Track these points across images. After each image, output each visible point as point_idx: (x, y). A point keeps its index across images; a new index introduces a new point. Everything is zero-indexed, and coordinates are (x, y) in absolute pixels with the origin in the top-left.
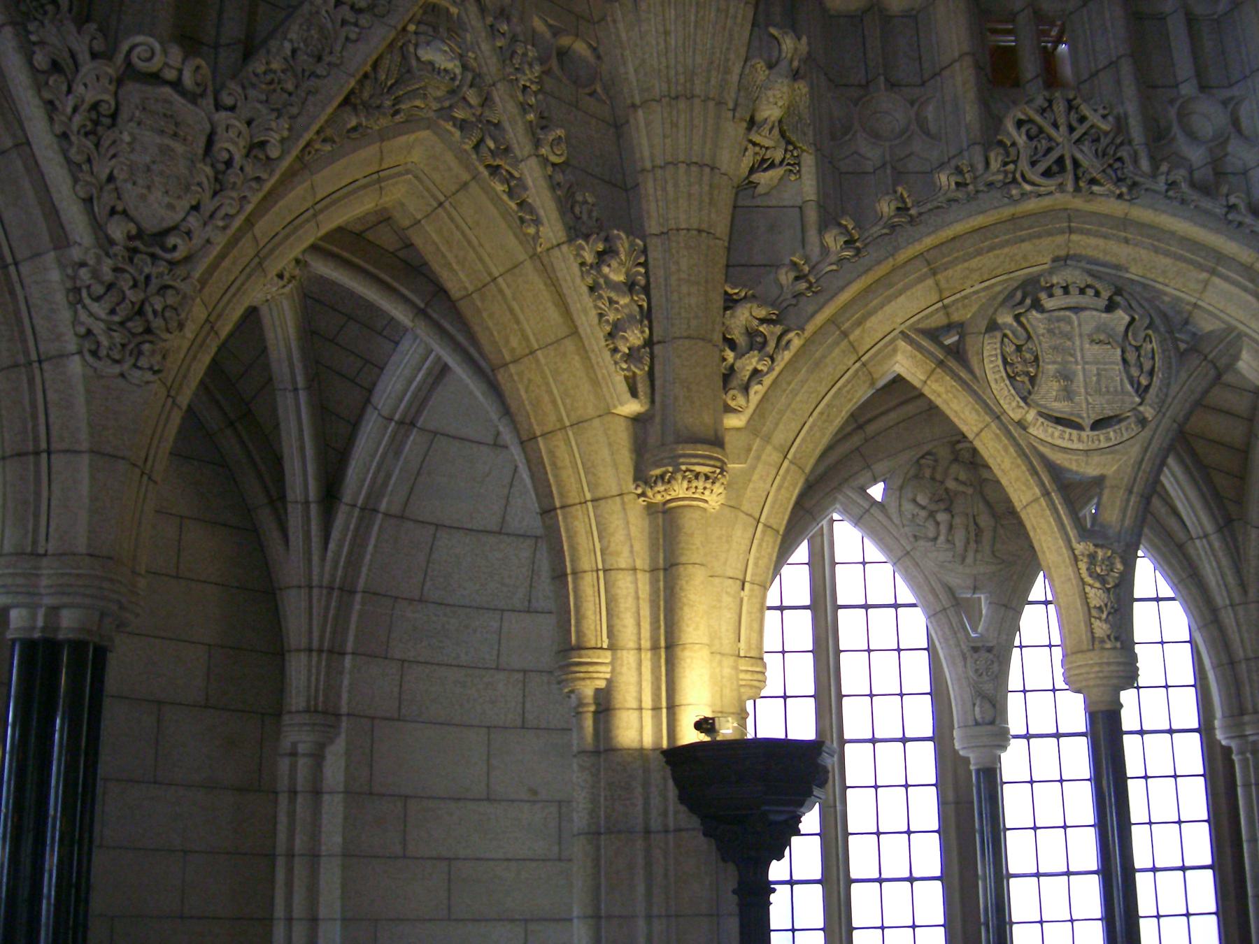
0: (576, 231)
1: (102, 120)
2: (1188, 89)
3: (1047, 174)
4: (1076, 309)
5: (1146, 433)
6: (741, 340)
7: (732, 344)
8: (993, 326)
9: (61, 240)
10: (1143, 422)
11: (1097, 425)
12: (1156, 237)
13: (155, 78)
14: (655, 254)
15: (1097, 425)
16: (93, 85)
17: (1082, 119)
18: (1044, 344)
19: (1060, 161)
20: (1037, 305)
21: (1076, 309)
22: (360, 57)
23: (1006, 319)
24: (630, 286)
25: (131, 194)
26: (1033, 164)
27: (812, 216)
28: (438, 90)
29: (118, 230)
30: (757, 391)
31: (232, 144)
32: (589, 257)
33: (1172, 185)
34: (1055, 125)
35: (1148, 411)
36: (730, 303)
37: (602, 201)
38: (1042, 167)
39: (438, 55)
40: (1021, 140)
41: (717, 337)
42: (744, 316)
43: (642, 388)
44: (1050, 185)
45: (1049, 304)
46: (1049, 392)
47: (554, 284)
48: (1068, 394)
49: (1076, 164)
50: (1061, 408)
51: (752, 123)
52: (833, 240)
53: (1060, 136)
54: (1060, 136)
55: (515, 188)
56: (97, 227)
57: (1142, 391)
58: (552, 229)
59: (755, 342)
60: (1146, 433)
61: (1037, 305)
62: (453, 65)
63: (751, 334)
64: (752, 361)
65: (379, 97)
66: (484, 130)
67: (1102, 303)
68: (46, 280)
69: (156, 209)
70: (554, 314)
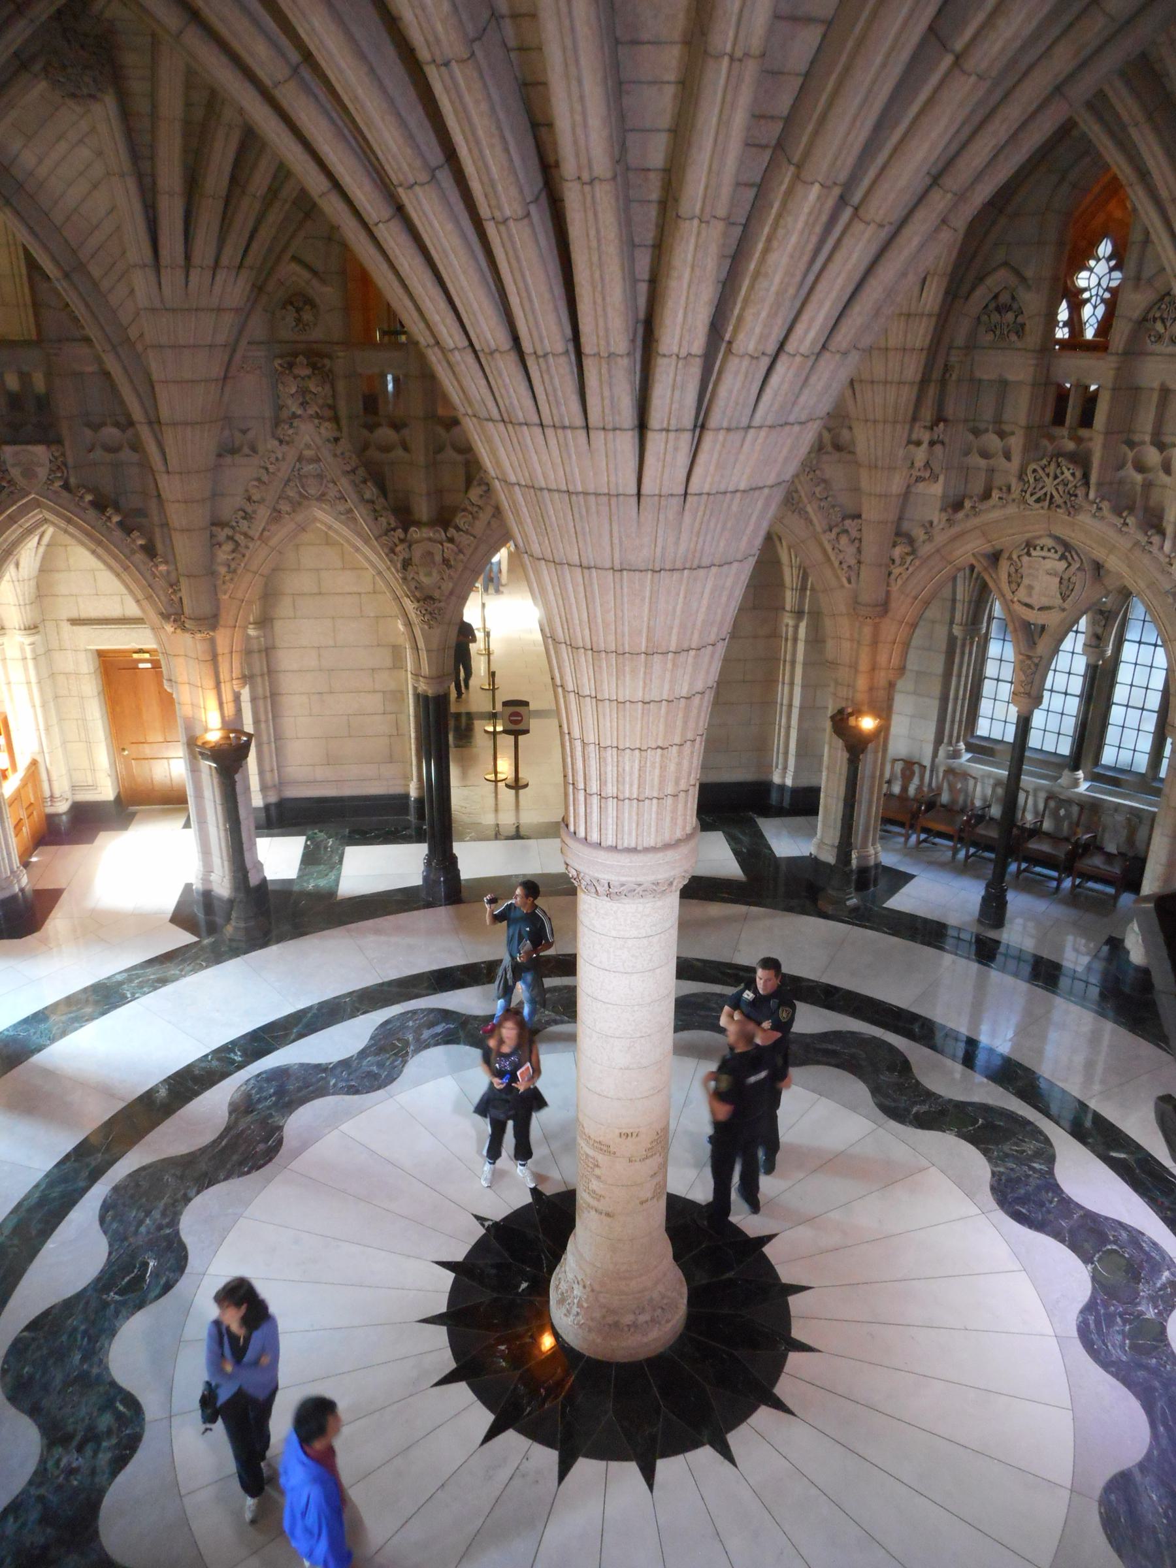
2: (1147, 438)
3: (1038, 501)
4: (1044, 558)
6: (898, 561)
7: (893, 561)
8: (1010, 558)
10: (1064, 610)
11: (1040, 609)
15: (1039, 609)
17: (1062, 473)
18: (1024, 571)
19: (1045, 494)
20: (1028, 554)
21: (1044, 558)
23: (1015, 557)
26: (1032, 495)
27: (938, 505)
32: (833, 535)
34: (1048, 475)
35: (1066, 605)
38: (1035, 497)
40: (1032, 480)
44: (1038, 506)
45: (1034, 553)
46: (1022, 594)
48: (1030, 595)
49: (1052, 497)
50: (1028, 600)
52: (944, 516)
53: (1048, 481)
54: (1048, 481)
61: (1028, 554)
67: (1057, 556)
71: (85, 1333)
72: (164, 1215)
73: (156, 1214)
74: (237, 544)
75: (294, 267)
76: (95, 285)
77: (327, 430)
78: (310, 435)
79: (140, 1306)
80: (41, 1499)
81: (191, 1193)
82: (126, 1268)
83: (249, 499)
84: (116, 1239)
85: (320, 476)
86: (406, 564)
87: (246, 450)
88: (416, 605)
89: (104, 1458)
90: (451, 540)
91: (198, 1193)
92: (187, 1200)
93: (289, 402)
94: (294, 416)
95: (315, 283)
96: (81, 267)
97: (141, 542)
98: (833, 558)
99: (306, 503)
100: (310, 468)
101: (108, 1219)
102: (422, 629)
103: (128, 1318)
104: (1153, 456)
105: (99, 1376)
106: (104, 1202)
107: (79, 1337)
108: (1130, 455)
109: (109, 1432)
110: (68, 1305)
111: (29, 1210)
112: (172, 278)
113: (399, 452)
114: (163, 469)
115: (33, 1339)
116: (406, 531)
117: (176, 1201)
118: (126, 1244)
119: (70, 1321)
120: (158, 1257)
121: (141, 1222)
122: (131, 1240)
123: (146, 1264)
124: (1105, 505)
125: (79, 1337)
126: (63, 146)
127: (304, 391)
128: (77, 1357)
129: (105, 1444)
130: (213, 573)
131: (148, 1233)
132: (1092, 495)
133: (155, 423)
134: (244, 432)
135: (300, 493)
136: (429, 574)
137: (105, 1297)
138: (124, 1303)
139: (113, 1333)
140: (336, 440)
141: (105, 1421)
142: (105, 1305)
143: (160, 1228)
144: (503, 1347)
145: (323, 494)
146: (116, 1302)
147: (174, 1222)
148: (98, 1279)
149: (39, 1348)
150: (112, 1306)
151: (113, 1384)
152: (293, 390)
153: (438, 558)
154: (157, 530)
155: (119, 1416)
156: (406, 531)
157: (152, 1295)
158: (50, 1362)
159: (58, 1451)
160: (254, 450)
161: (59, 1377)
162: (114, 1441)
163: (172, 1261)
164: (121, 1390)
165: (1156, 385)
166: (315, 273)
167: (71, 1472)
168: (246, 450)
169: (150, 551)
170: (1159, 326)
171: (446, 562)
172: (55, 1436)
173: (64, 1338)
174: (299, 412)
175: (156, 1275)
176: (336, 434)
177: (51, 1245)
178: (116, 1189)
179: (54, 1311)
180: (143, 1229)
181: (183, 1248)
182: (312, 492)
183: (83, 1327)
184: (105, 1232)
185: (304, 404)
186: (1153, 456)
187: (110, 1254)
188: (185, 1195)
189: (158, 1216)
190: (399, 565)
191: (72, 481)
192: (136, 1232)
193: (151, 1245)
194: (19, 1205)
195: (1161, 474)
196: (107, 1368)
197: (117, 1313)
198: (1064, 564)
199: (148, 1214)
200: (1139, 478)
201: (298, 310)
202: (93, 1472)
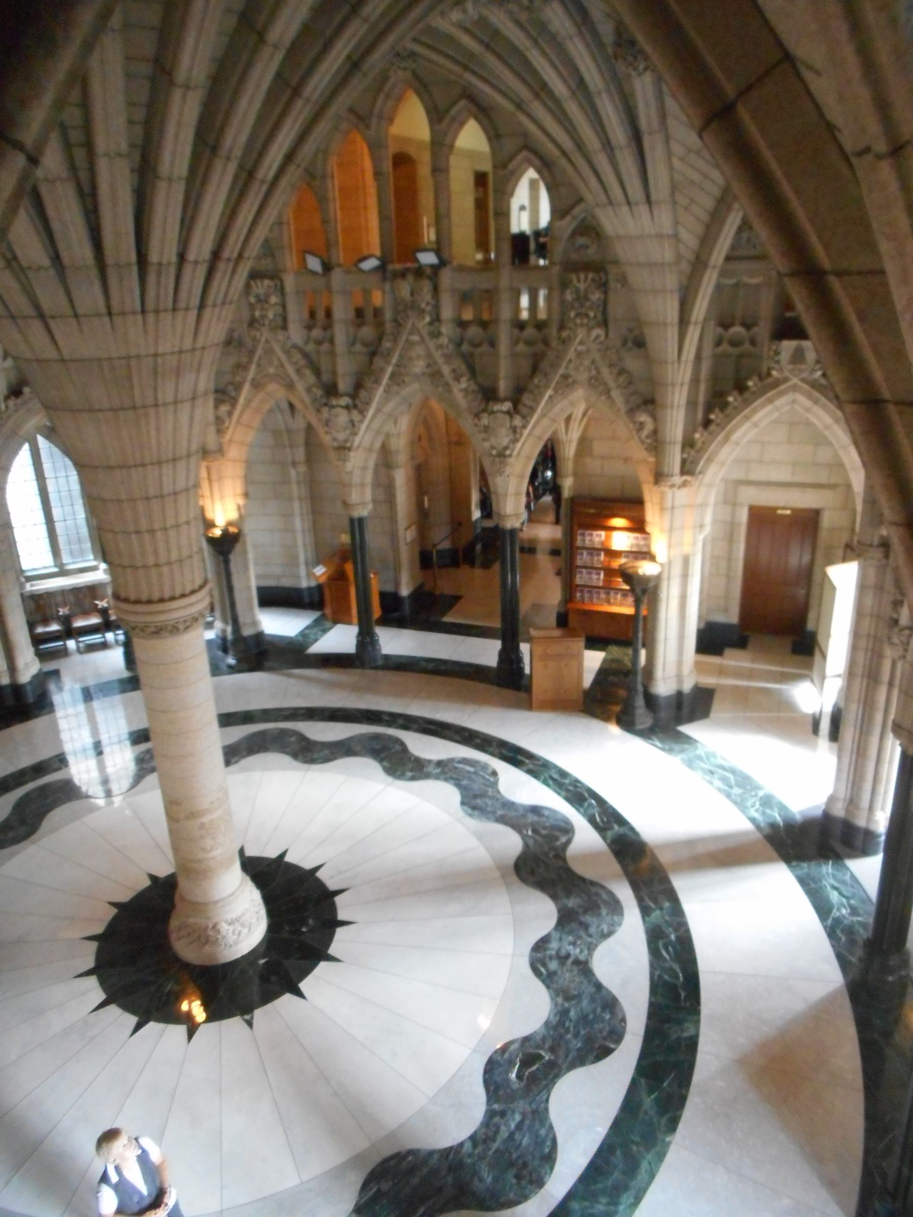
71: (567, 1031)
72: (497, 1132)
73: (504, 1133)
79: (526, 1039)
80: (590, 936)
81: (468, 1146)
82: (534, 1080)
84: (540, 1115)
89: (554, 945)
91: (461, 1144)
92: (473, 1138)
101: (549, 1143)
103: (535, 1032)
105: (557, 995)
106: (552, 1169)
107: (572, 1029)
109: (551, 958)
110: (581, 1060)
111: (626, 1188)
115: (605, 1039)
117: (485, 1141)
118: (534, 1106)
119: (579, 1045)
120: (507, 1081)
121: (519, 1126)
122: (529, 1110)
123: (519, 1077)
125: (572, 1029)
128: (572, 1014)
129: (553, 953)
131: (513, 1112)
137: (552, 1058)
138: (538, 1047)
139: (547, 1024)
141: (553, 965)
142: (552, 1050)
143: (503, 1114)
144: (304, 930)
146: (543, 1049)
147: (490, 1114)
148: (557, 1076)
149: (601, 1031)
150: (547, 1046)
151: (548, 987)
155: (544, 965)
157: (515, 1046)
158: (591, 1017)
159: (582, 957)
161: (585, 1003)
162: (548, 953)
163: (497, 1072)
164: (543, 981)
167: (574, 944)
172: (584, 968)
173: (583, 1032)
175: (511, 1063)
177: (601, 1130)
178: (540, 1183)
179: (591, 1058)
180: (518, 1117)
181: (487, 1083)
183: (569, 1036)
184: (551, 1127)
187: (547, 1100)
188: (475, 1146)
189: (503, 1128)
192: (524, 1115)
193: (511, 1097)
194: (638, 1199)
196: (552, 999)
197: (544, 1039)
199: (511, 1136)
202: (561, 939)
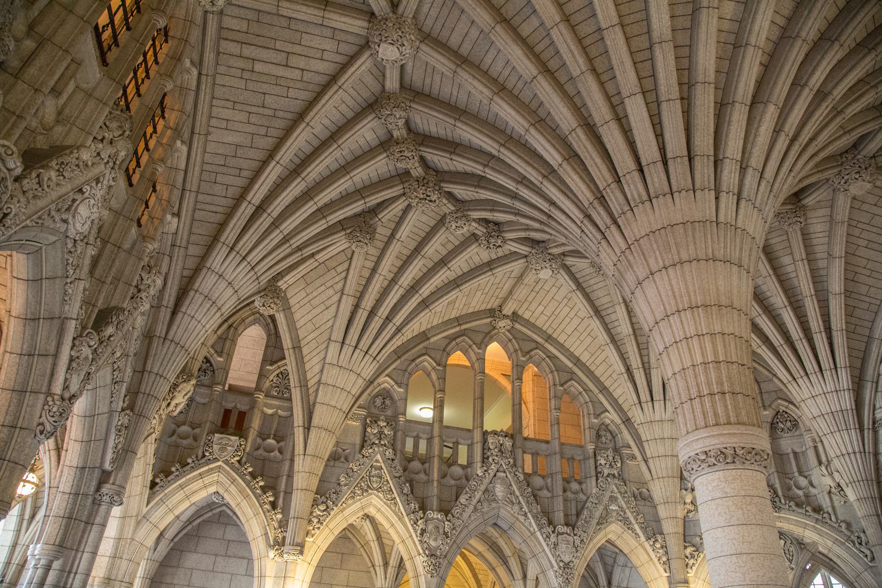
0: (648, 539)
1: (556, 545)
2: (796, 474)
5: (794, 572)
9: (552, 567)
10: (792, 569)
12: (788, 520)
13: (563, 533)
14: (667, 539)
16: (553, 538)
22: (597, 514)
24: (662, 547)
25: (562, 557)
28: (614, 514)
29: (561, 564)
30: (694, 568)
31: (578, 542)
32: (652, 543)
33: (790, 506)
36: (685, 547)
37: (653, 530)
39: (613, 507)
41: (683, 557)
42: (689, 550)
43: (668, 570)
47: (645, 550)
51: (685, 503)
55: (633, 530)
56: (558, 564)
57: (791, 561)
58: (643, 539)
59: (692, 556)
60: (794, 572)
62: (617, 508)
63: (691, 554)
64: (691, 562)
65: (603, 521)
66: (626, 521)
68: (551, 574)
69: (567, 559)
70: (646, 556)
74: (328, 507)
75: (387, 378)
76: (303, 358)
77: (389, 453)
78: (378, 457)
83: (339, 484)
85: (381, 477)
86: (423, 531)
87: (342, 459)
88: (426, 559)
90: (449, 521)
93: (372, 437)
94: (373, 444)
95: (396, 387)
96: (300, 348)
97: (272, 499)
98: (653, 557)
99: (370, 491)
100: (374, 472)
102: (426, 578)
104: (803, 482)
108: (792, 482)
112: (347, 350)
113: (422, 476)
114: (302, 452)
116: (424, 513)
124: (792, 503)
126: (323, 288)
127: (381, 433)
130: (310, 521)
132: (783, 501)
133: (307, 428)
134: (344, 451)
135: (368, 486)
136: (435, 540)
140: (393, 460)
145: (380, 488)
152: (375, 431)
153: (441, 531)
154: (282, 494)
156: (424, 513)
160: (347, 459)
165: (789, 451)
166: (396, 383)
168: (342, 459)
169: (274, 505)
170: (780, 425)
171: (445, 534)
174: (377, 442)
176: (393, 457)
182: (375, 486)
185: (380, 439)
186: (803, 482)
190: (419, 532)
191: (244, 460)
195: (811, 489)
198: (782, 542)
200: (800, 493)
201: (384, 399)
